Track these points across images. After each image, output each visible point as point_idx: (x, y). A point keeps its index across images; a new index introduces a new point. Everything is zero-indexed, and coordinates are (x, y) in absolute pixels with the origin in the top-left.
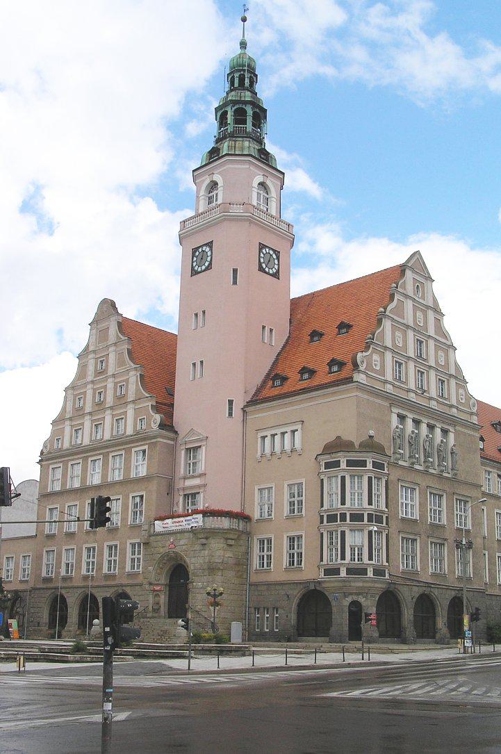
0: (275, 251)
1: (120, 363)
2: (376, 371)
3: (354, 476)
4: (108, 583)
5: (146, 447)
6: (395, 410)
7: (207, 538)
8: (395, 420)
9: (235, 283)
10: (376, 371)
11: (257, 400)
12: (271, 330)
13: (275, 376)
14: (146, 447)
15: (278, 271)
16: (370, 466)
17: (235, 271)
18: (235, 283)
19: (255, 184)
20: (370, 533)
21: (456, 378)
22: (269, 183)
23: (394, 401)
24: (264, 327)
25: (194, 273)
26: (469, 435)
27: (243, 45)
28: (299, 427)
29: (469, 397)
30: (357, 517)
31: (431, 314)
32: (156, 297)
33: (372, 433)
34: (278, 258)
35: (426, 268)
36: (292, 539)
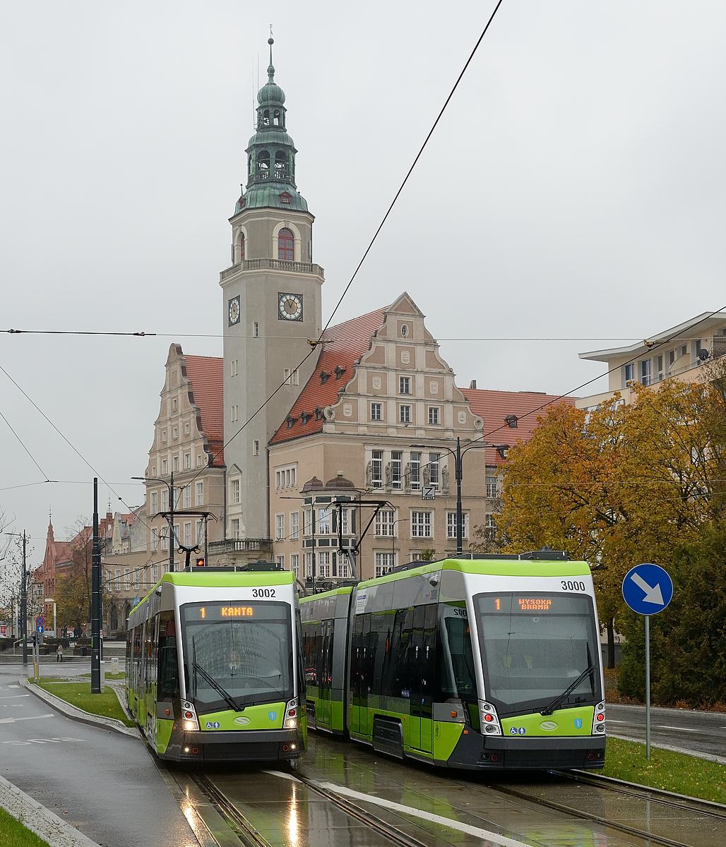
0: (296, 295)
5: (202, 481)
7: (235, 559)
8: (369, 458)
10: (348, 419)
11: (276, 440)
13: (290, 420)
14: (202, 481)
19: (276, 233)
23: (365, 439)
25: (231, 324)
27: (271, 72)
28: (295, 466)
30: (324, 542)
31: (421, 352)
32: (207, 342)
33: (339, 472)
35: (415, 306)
36: (294, 556)
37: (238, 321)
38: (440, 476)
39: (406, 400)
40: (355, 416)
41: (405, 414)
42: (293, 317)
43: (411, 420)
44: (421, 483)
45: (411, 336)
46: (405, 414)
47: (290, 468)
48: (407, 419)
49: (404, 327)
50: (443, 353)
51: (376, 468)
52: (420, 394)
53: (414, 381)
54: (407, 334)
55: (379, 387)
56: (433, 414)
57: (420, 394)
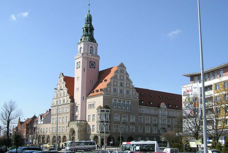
1: (64, 87)
2: (109, 91)
4: (63, 134)
6: (113, 99)
8: (113, 101)
10: (109, 91)
14: (68, 106)
16: (105, 111)
17: (84, 68)
33: (107, 104)
34: (95, 64)
37: (79, 67)
40: (110, 91)
41: (121, 91)
43: (123, 93)
45: (123, 73)
47: (93, 103)
48: (122, 93)
50: (130, 77)
52: (125, 86)
56: (128, 92)
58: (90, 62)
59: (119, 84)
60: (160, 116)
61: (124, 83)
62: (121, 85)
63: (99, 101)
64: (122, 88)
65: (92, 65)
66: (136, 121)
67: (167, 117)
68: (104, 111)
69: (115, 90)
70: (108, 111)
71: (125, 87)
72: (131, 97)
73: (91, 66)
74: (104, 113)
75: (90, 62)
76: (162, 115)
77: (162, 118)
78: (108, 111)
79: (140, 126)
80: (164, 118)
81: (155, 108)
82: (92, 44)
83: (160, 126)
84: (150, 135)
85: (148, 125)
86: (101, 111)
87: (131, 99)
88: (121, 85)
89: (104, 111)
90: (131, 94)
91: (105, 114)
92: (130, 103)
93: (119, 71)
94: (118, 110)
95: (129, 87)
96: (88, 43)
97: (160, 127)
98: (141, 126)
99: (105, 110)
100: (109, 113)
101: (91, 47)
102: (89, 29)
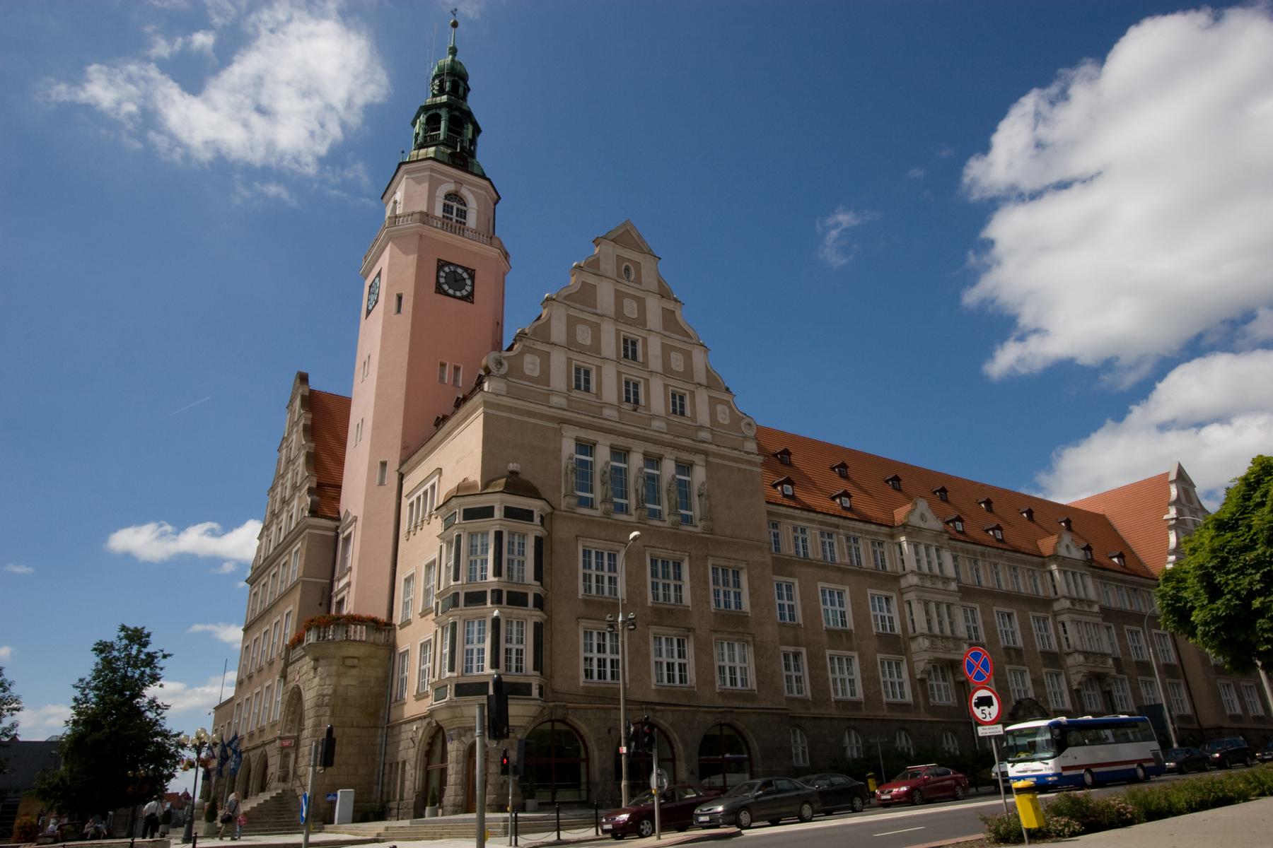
3: (476, 534)
8: (568, 447)
9: (399, 311)
12: (457, 369)
15: (471, 294)
16: (498, 514)
17: (400, 298)
18: (399, 311)
20: (496, 622)
21: (707, 387)
22: (465, 192)
24: (443, 365)
26: (739, 469)
29: (737, 418)
34: (472, 278)
38: (696, 502)
39: (632, 372)
40: (545, 377)
41: (631, 393)
42: (458, 294)
44: (664, 507)
45: (638, 280)
46: (631, 393)
48: (637, 402)
49: (627, 269)
51: (583, 472)
52: (656, 363)
53: (645, 345)
54: (633, 277)
55: (588, 342)
56: (677, 404)
57: (656, 363)
58: (441, 264)
59: (609, 345)
60: (914, 580)
61: (645, 340)
62: (629, 350)
63: (461, 455)
64: (632, 372)
65: (456, 281)
66: (753, 606)
67: (953, 586)
68: (487, 512)
69: (581, 379)
70: (526, 515)
71: (660, 369)
72: (704, 435)
73: (446, 287)
74: (491, 526)
75: (441, 264)
76: (921, 575)
77: (927, 596)
78: (526, 515)
79: (791, 649)
80: (939, 598)
81: (875, 533)
82: (459, 182)
83: (922, 651)
84: (865, 713)
85: (839, 637)
86: (470, 514)
87: (706, 453)
88: (629, 350)
89: (487, 512)
90: (703, 417)
91: (499, 535)
92: (699, 475)
93: (608, 267)
94: (607, 514)
95: (688, 375)
96: (432, 170)
97: (926, 656)
98: (797, 645)
99: (498, 501)
100: (533, 530)
101: (453, 196)
102: (444, 113)
